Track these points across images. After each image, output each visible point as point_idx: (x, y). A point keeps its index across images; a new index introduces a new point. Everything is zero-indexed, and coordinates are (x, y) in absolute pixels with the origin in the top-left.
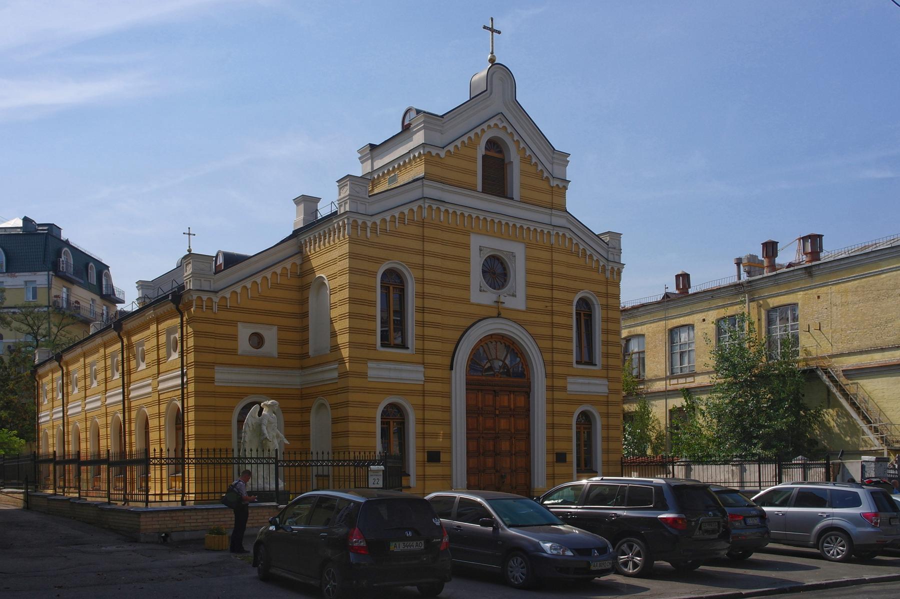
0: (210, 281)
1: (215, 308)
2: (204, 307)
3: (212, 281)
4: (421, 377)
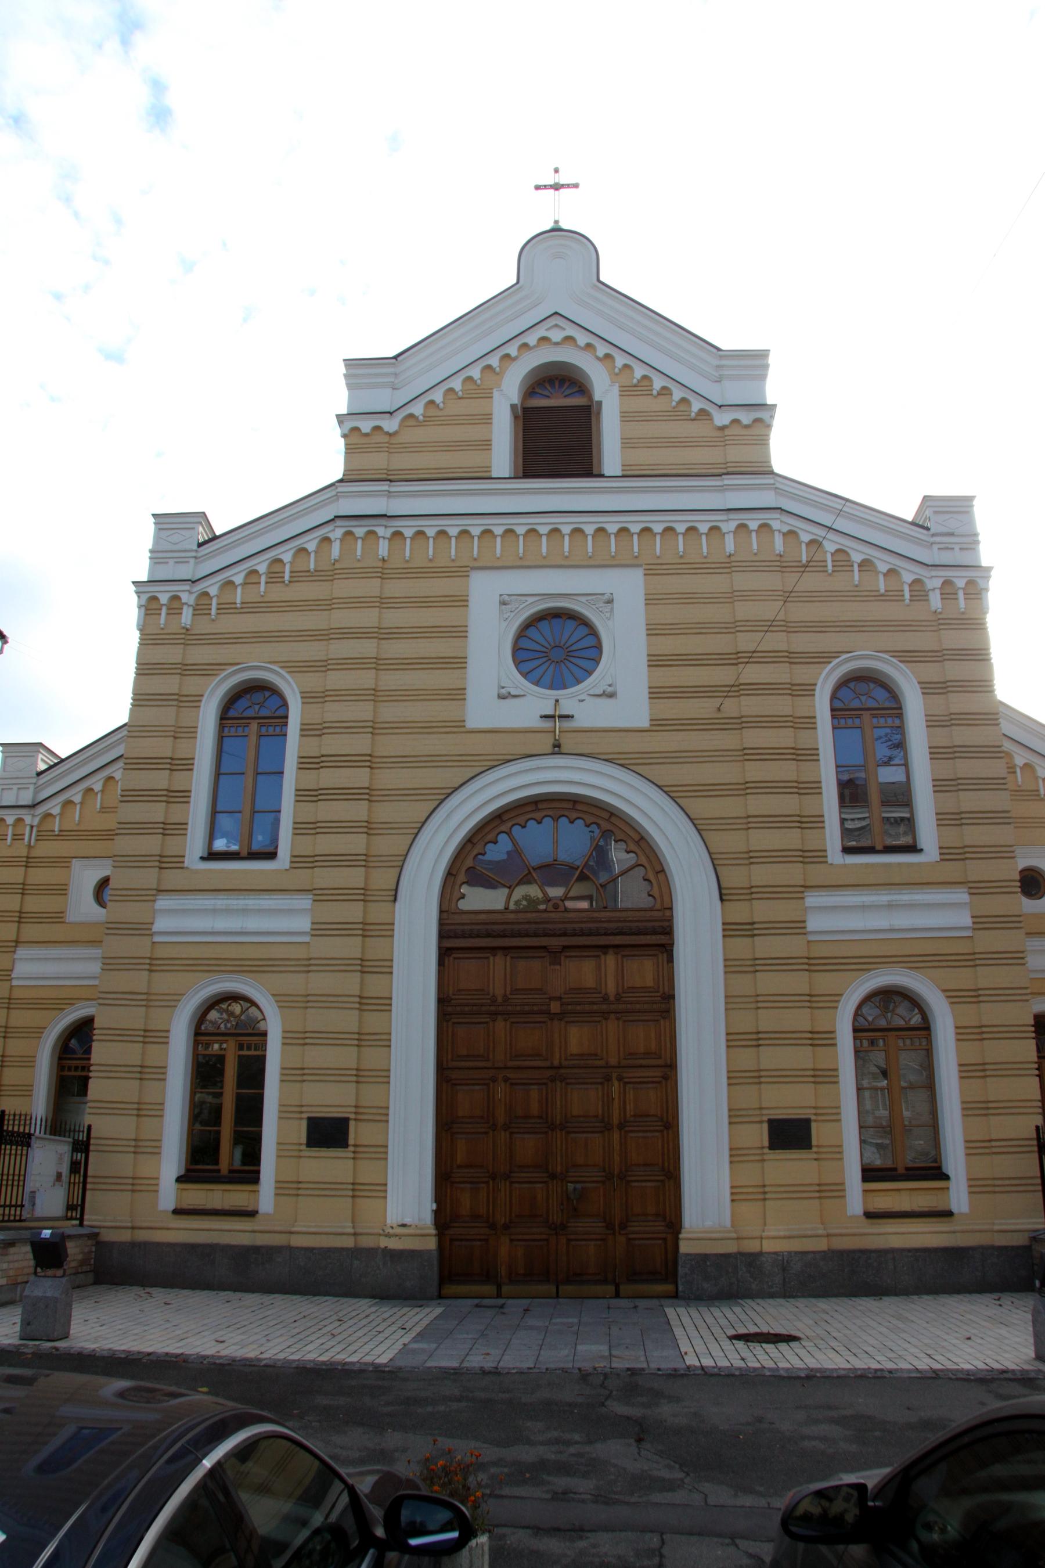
2: (9, 838)
4: (304, 924)
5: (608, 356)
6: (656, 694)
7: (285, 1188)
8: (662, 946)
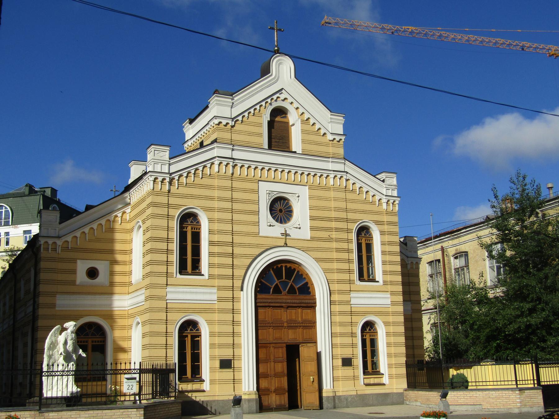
0: (56, 229)
1: (59, 250)
3: (57, 229)
5: (297, 108)
6: (312, 229)
7: (212, 382)
8: (313, 307)
